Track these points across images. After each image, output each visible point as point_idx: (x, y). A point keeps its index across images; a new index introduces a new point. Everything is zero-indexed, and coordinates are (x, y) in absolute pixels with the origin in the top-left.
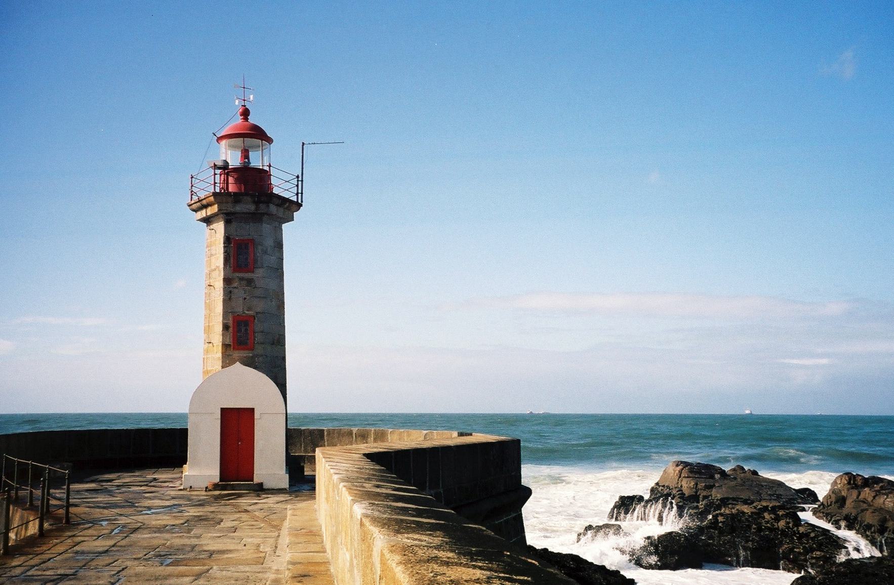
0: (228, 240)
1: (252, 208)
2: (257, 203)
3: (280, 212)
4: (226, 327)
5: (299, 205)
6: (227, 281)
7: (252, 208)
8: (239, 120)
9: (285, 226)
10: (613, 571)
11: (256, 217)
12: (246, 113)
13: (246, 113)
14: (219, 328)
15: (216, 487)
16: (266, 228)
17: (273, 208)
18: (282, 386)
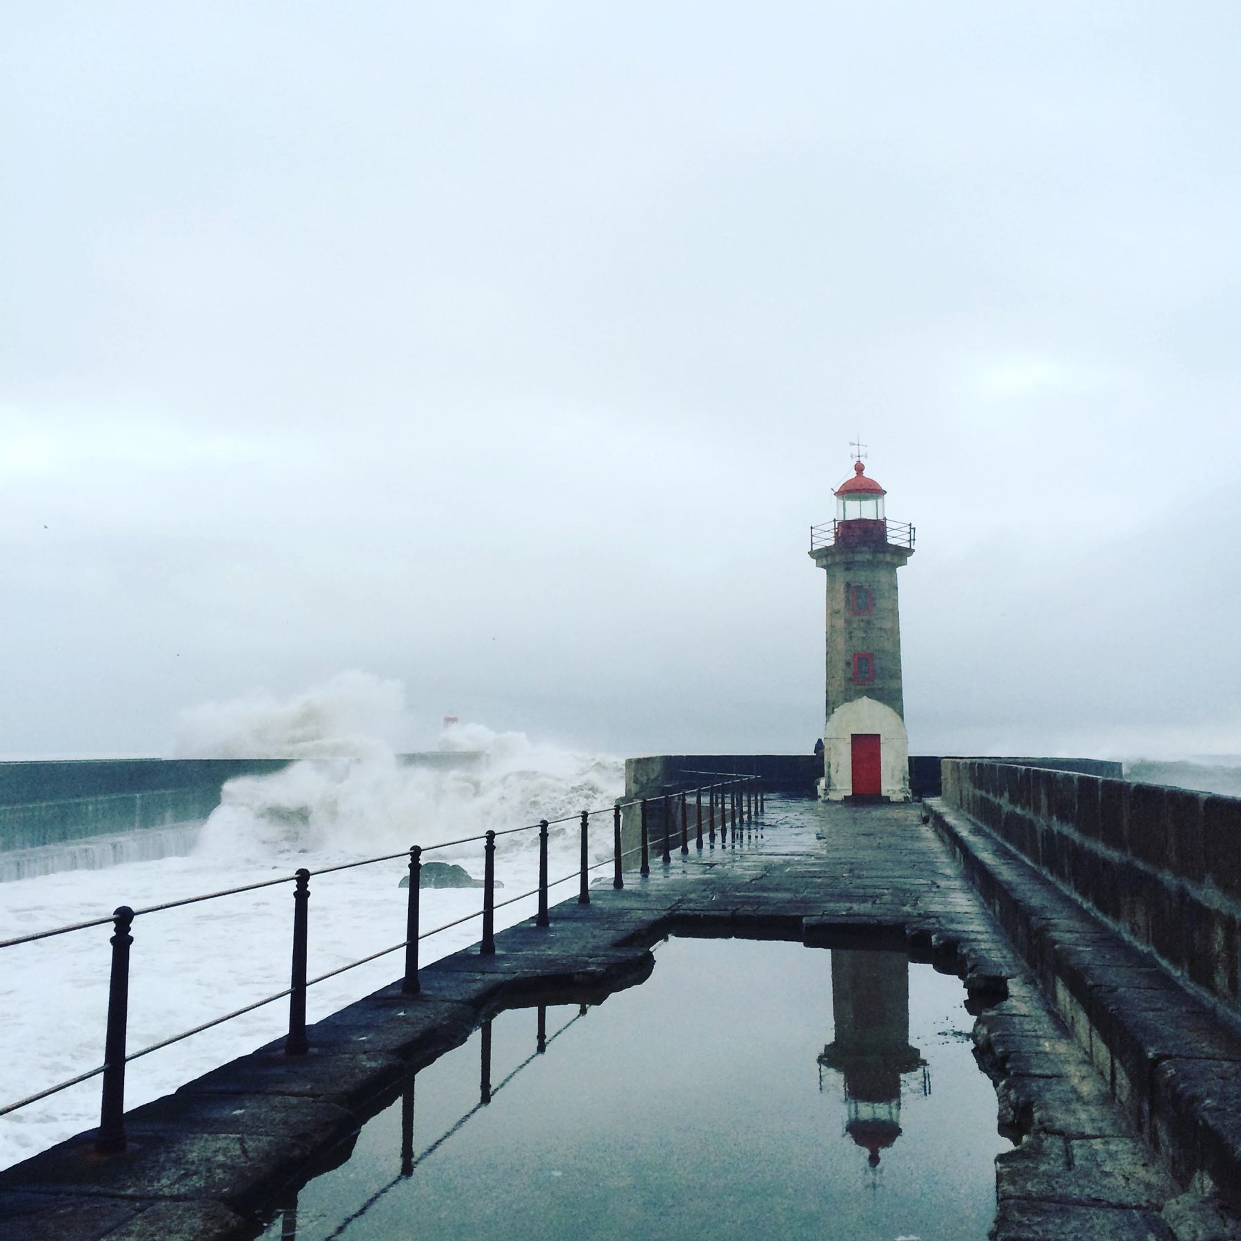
0: (848, 585)
1: (869, 557)
3: (896, 560)
4: (848, 664)
5: (910, 551)
6: (848, 622)
7: (869, 557)
8: (853, 474)
9: (899, 569)
11: (873, 565)
12: (859, 468)
13: (859, 468)
14: (841, 665)
16: (882, 576)
17: (888, 558)
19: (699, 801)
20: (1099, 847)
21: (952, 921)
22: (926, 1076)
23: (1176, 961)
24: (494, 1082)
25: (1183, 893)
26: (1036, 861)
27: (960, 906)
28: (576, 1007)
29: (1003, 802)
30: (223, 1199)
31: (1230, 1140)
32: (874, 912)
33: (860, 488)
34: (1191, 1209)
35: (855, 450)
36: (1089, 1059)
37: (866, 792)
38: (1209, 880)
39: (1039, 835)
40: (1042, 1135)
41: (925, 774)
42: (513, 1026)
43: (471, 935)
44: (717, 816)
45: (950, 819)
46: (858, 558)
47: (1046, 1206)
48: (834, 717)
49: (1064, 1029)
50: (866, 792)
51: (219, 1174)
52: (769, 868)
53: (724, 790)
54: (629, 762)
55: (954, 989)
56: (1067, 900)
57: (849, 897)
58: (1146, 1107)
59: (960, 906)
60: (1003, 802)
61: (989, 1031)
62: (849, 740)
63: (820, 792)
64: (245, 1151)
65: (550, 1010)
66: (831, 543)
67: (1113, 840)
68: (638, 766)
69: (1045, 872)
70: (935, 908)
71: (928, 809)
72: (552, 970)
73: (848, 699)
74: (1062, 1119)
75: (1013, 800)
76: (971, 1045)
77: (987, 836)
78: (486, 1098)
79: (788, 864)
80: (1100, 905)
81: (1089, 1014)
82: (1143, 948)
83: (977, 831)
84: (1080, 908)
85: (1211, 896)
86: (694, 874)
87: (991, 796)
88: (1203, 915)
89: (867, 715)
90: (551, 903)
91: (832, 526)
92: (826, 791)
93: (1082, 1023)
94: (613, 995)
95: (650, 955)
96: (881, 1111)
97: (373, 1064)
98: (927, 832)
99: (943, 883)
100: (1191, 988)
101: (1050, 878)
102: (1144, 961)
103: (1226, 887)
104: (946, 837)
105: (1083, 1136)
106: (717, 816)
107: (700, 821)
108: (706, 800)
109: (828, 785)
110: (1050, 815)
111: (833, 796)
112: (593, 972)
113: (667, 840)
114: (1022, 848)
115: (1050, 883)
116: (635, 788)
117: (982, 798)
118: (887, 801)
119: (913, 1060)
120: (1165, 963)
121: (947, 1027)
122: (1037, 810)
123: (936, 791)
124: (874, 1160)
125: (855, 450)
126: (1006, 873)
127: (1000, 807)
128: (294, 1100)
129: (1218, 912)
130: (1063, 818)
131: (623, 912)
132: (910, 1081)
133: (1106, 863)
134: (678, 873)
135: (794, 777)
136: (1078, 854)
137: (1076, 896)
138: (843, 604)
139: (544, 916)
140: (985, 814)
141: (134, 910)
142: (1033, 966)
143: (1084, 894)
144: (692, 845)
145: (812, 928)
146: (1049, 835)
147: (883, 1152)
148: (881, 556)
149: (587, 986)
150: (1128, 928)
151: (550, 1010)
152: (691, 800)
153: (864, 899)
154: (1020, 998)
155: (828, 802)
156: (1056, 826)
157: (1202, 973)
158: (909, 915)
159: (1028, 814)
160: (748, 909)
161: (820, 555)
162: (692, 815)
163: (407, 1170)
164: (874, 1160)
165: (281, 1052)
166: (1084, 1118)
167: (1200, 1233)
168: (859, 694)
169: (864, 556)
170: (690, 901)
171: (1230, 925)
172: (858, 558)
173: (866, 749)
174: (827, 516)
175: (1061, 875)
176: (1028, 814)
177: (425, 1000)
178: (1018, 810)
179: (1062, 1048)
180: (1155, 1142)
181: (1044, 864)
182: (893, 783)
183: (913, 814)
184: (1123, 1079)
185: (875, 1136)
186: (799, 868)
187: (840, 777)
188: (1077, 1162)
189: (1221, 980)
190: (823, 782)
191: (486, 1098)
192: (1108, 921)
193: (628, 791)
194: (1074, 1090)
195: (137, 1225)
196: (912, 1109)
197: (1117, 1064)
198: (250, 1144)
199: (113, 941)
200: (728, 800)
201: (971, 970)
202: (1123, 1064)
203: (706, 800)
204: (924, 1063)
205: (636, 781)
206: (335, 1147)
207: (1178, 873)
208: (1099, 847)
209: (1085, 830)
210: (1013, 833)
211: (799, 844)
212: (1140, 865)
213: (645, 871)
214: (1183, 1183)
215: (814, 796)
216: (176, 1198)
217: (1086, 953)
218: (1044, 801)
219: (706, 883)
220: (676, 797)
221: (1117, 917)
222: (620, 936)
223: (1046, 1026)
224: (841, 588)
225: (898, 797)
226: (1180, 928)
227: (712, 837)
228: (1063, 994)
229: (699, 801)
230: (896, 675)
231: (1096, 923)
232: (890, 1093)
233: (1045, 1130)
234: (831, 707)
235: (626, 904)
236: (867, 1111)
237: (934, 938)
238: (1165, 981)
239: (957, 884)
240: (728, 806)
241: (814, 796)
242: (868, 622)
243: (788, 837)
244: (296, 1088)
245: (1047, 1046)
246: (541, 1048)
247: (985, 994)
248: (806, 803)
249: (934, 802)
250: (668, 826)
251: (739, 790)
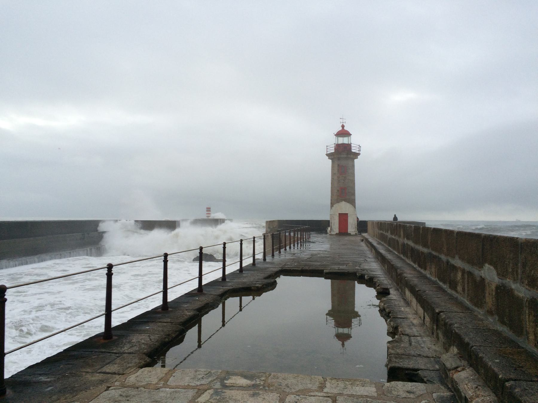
0: (338, 165)
1: (345, 156)
2: (347, 154)
4: (338, 191)
5: (359, 154)
7: (345, 156)
8: (341, 129)
9: (355, 160)
10: (518, 298)
12: (343, 126)
13: (343, 126)
14: (336, 191)
15: (337, 234)
17: (352, 156)
18: (355, 207)
19: (290, 234)
20: (420, 248)
21: (372, 271)
22: (360, 320)
23: (445, 283)
24: (226, 320)
25: (448, 262)
26: (399, 253)
27: (374, 267)
28: (251, 297)
29: (389, 235)
30: (144, 354)
31: (463, 336)
32: (347, 268)
33: (343, 133)
34: (451, 357)
35: (341, 120)
36: (416, 313)
37: (343, 232)
38: (457, 257)
39: (400, 244)
40: (402, 335)
41: (362, 226)
42: (232, 302)
43: (219, 275)
44: (296, 239)
45: (370, 240)
46: (342, 156)
47: (403, 356)
48: (333, 208)
49: (408, 304)
50: (343, 232)
51: (143, 346)
52: (312, 255)
53: (298, 231)
54: (267, 222)
55: (373, 292)
56: (409, 264)
57: (339, 264)
58: (435, 327)
59: (374, 267)
60: (389, 235)
61: (384, 304)
62: (338, 215)
63: (328, 232)
64: (150, 339)
65: (243, 298)
66: (333, 151)
67: (425, 245)
68: (270, 223)
69: (402, 256)
70: (366, 267)
71: (363, 237)
72: (245, 286)
73: (339, 202)
74: (408, 331)
75: (392, 234)
76: (378, 309)
77: (383, 245)
78: (224, 325)
79: (319, 254)
80: (419, 266)
81: (417, 299)
82: (433, 278)
83: (379, 243)
84: (413, 267)
85: (457, 262)
86: (289, 257)
87: (384, 233)
88: (454, 268)
89: (344, 207)
90: (244, 265)
91: (333, 146)
92: (330, 232)
93: (414, 302)
94: (264, 295)
95: (276, 281)
96: (346, 331)
97: (188, 314)
98: (363, 244)
99: (368, 260)
100: (449, 291)
101: (403, 258)
102: (434, 283)
103: (462, 259)
104: (369, 245)
105: (414, 336)
106: (296, 239)
107: (290, 240)
108: (292, 234)
109: (331, 229)
110: (404, 238)
111: (333, 233)
112: (257, 287)
113: (280, 246)
114: (394, 248)
115: (403, 259)
116: (269, 230)
117: (381, 233)
118: (350, 235)
119: (356, 315)
120: (441, 284)
121: (371, 303)
122: (400, 236)
123: (366, 231)
124: (343, 345)
125: (341, 120)
126: (389, 256)
127: (387, 236)
128: (165, 324)
129: (460, 268)
130: (408, 239)
131: (266, 269)
132: (355, 321)
133: (422, 253)
134: (284, 257)
135: (320, 227)
136: (412, 250)
137: (412, 263)
138: (337, 170)
139: (241, 269)
140: (382, 238)
141: (113, 264)
142: (398, 284)
143: (415, 263)
144: (288, 248)
145: (327, 273)
146: (404, 245)
147: (346, 343)
148: (349, 156)
149: (255, 291)
150: (429, 272)
151: (244, 298)
152: (287, 234)
153: (343, 264)
154: (394, 294)
155: (331, 235)
156: (406, 241)
157: (453, 285)
158: (358, 269)
159: (396, 238)
160: (307, 268)
161: (330, 155)
162: (288, 239)
163: (200, 346)
164: (343, 345)
165: (160, 310)
166: (415, 331)
167: (453, 364)
168: (342, 201)
169: (344, 156)
170: (288, 265)
171: (463, 271)
172: (342, 156)
173: (343, 218)
174: (332, 141)
175: (407, 257)
176: (396, 238)
177: (205, 294)
178: (393, 237)
179: (407, 309)
180: (438, 338)
181: (402, 253)
182: (352, 228)
183: (359, 238)
184: (427, 319)
185: (343, 338)
186: (322, 255)
187: (335, 228)
188: (413, 344)
189: (459, 288)
190: (329, 229)
191: (224, 325)
192: (422, 271)
193: (267, 231)
194: (412, 323)
195: (118, 361)
196: (355, 330)
197: (425, 314)
198: (152, 337)
199: (107, 274)
200: (299, 234)
201: (378, 286)
202: (428, 315)
203: (292, 234)
204: (359, 316)
205: (269, 228)
206: (177, 338)
207: (447, 255)
208: (420, 248)
209: (416, 242)
210: (391, 244)
211: (322, 248)
212: (434, 253)
213: (273, 255)
214: (447, 350)
215: (326, 233)
216: (130, 353)
217: (415, 281)
218: (402, 233)
219: (293, 259)
220: (282, 233)
221: (425, 269)
222: (266, 275)
223: (402, 303)
224: (336, 166)
225: (354, 233)
226: (446, 273)
227: (294, 245)
228: (408, 293)
229: (290, 234)
230: (354, 194)
231: (418, 271)
232: (348, 325)
233: (403, 334)
234: (332, 205)
235: (267, 266)
236: (341, 330)
237: (366, 276)
238: (440, 289)
239: (373, 260)
240: (299, 236)
241: (326, 233)
242: (345, 177)
243: (319, 246)
244: (165, 321)
245: (403, 309)
246: (241, 310)
247: (383, 293)
248: (324, 235)
249: (365, 235)
250: (280, 242)
251: (302, 231)
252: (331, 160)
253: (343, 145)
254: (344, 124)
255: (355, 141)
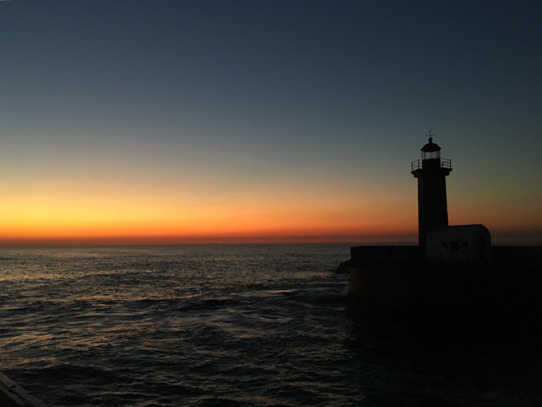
5: (451, 170)
9: (446, 177)
12: (430, 140)
13: (430, 140)
33: (431, 147)
174: (417, 158)
252: (417, 179)
253: (431, 160)
254: (432, 137)
255: (445, 156)
